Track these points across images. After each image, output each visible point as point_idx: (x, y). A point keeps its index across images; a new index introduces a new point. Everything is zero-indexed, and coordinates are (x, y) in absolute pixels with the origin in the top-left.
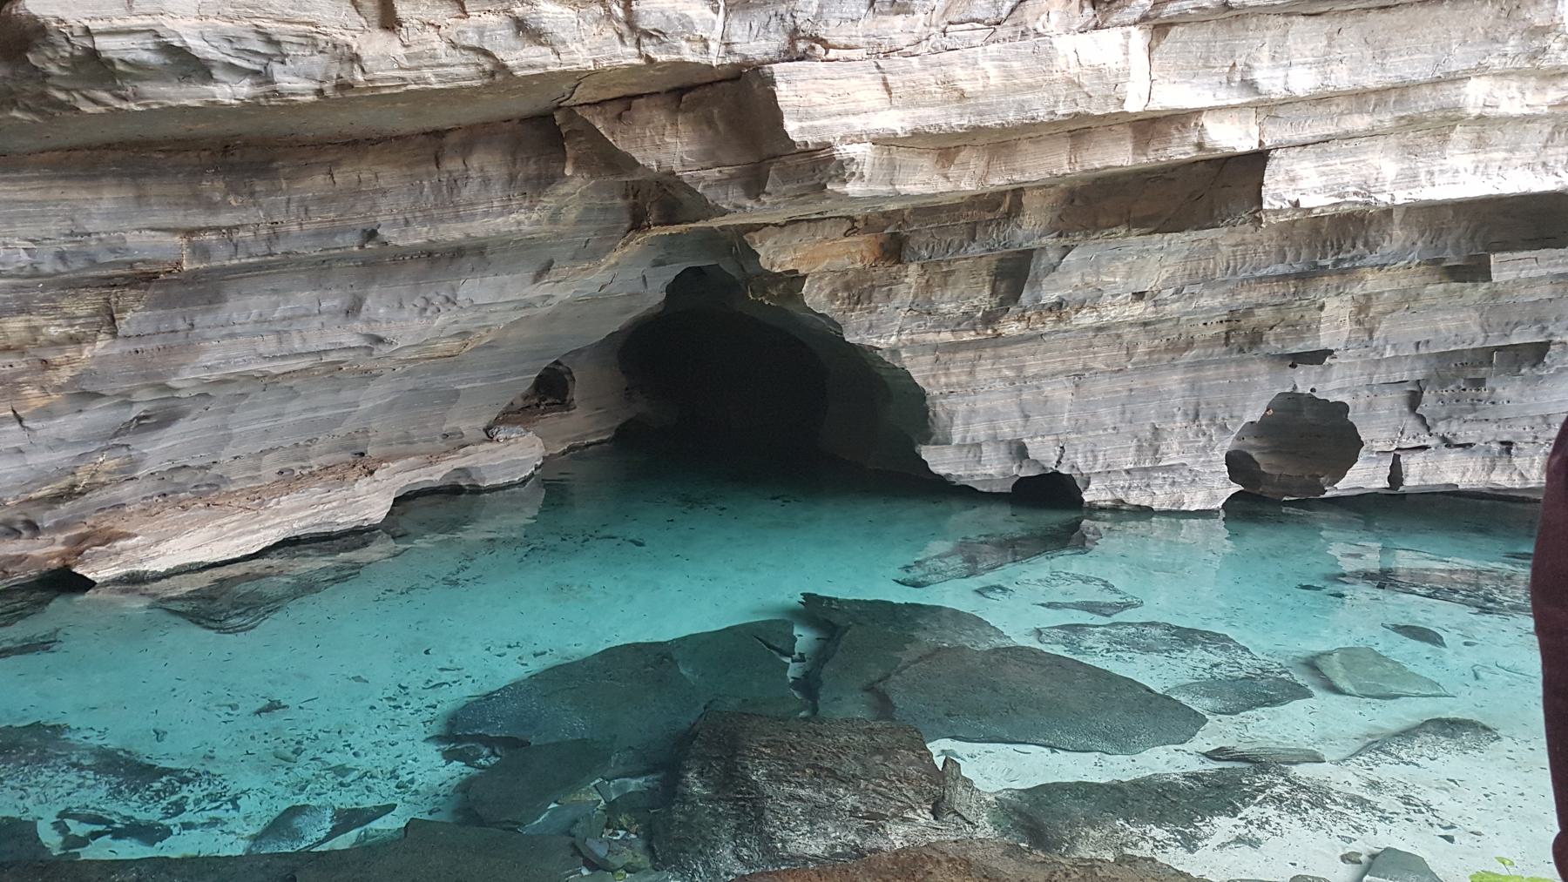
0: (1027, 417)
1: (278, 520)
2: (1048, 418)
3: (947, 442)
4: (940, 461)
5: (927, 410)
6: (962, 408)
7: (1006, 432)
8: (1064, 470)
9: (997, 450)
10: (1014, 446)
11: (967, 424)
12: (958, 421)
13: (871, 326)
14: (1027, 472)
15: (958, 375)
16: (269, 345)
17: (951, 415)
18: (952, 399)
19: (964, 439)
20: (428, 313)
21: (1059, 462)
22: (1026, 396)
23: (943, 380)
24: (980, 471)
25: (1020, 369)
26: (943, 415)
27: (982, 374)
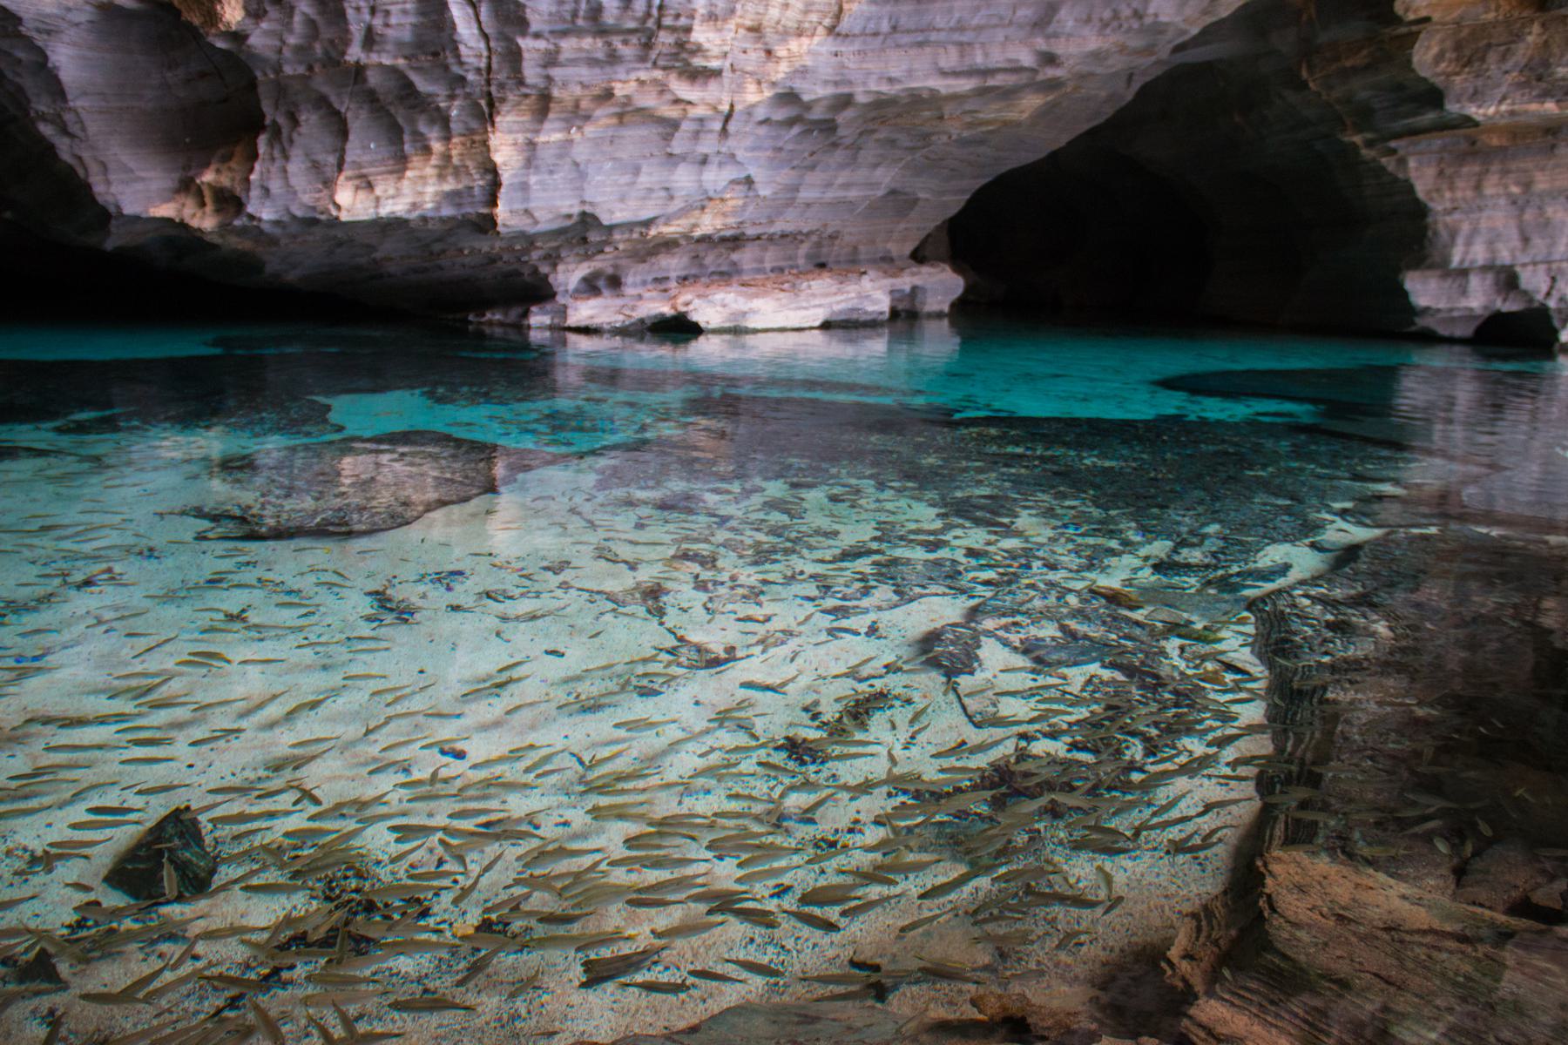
0: (1526, 240)
1: (817, 302)
2: (1548, 241)
3: (1443, 268)
4: (1423, 290)
5: (1426, 228)
6: (1465, 228)
7: (1504, 257)
8: (1552, 304)
9: (1484, 279)
10: (1503, 276)
11: (1469, 243)
12: (1460, 241)
13: (1476, 92)
14: (1511, 306)
15: (1463, 191)
16: (950, 59)
17: (1453, 234)
18: (1457, 216)
19: (1462, 261)
20: (1108, 31)
21: (1548, 294)
22: (1529, 216)
23: (1448, 195)
24: (1464, 303)
25: (1527, 186)
26: (1444, 234)
27: (1489, 190)
